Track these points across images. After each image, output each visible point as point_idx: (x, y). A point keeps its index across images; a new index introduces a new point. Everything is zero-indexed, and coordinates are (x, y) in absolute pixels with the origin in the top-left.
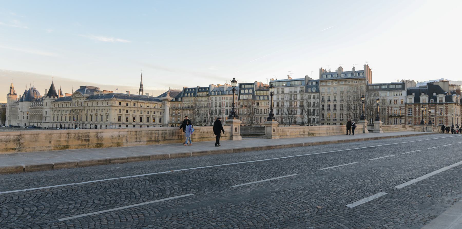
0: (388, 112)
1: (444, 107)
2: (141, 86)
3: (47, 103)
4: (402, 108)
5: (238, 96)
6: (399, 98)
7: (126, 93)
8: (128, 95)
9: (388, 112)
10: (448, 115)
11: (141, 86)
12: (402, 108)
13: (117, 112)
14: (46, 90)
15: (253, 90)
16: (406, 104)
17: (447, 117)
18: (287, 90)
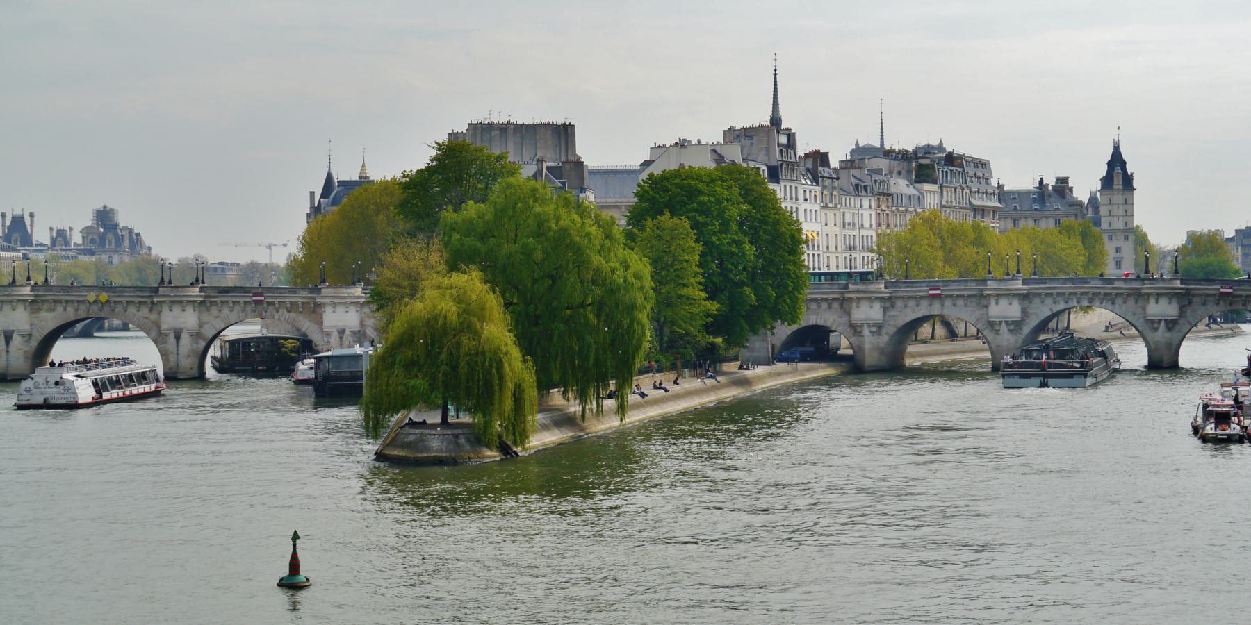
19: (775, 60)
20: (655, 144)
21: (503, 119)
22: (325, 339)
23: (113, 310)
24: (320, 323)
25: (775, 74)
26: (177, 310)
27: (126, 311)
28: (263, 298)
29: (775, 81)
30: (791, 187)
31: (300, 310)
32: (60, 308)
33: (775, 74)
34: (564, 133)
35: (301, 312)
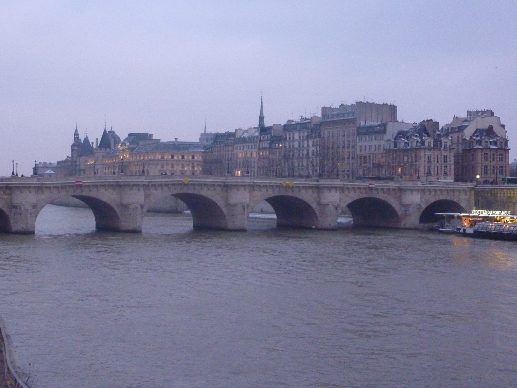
0: (373, 160)
1: (414, 153)
2: (262, 118)
3: (97, 157)
4: (384, 155)
5: (258, 144)
6: (383, 143)
7: (174, 140)
8: (175, 144)
9: (373, 160)
10: (418, 163)
11: (262, 118)
12: (384, 155)
13: (159, 167)
14: (97, 139)
15: (271, 136)
16: (386, 150)
17: (416, 165)
18: (296, 135)
19: (262, 92)
20: (455, 116)
21: (370, 101)
22: (403, 209)
23: (293, 192)
24: (400, 198)
25: (262, 98)
26: (333, 192)
27: (300, 192)
28: (374, 186)
29: (262, 102)
30: (252, 146)
31: (390, 193)
32: (264, 190)
33: (262, 98)
34: (393, 109)
35: (390, 194)
